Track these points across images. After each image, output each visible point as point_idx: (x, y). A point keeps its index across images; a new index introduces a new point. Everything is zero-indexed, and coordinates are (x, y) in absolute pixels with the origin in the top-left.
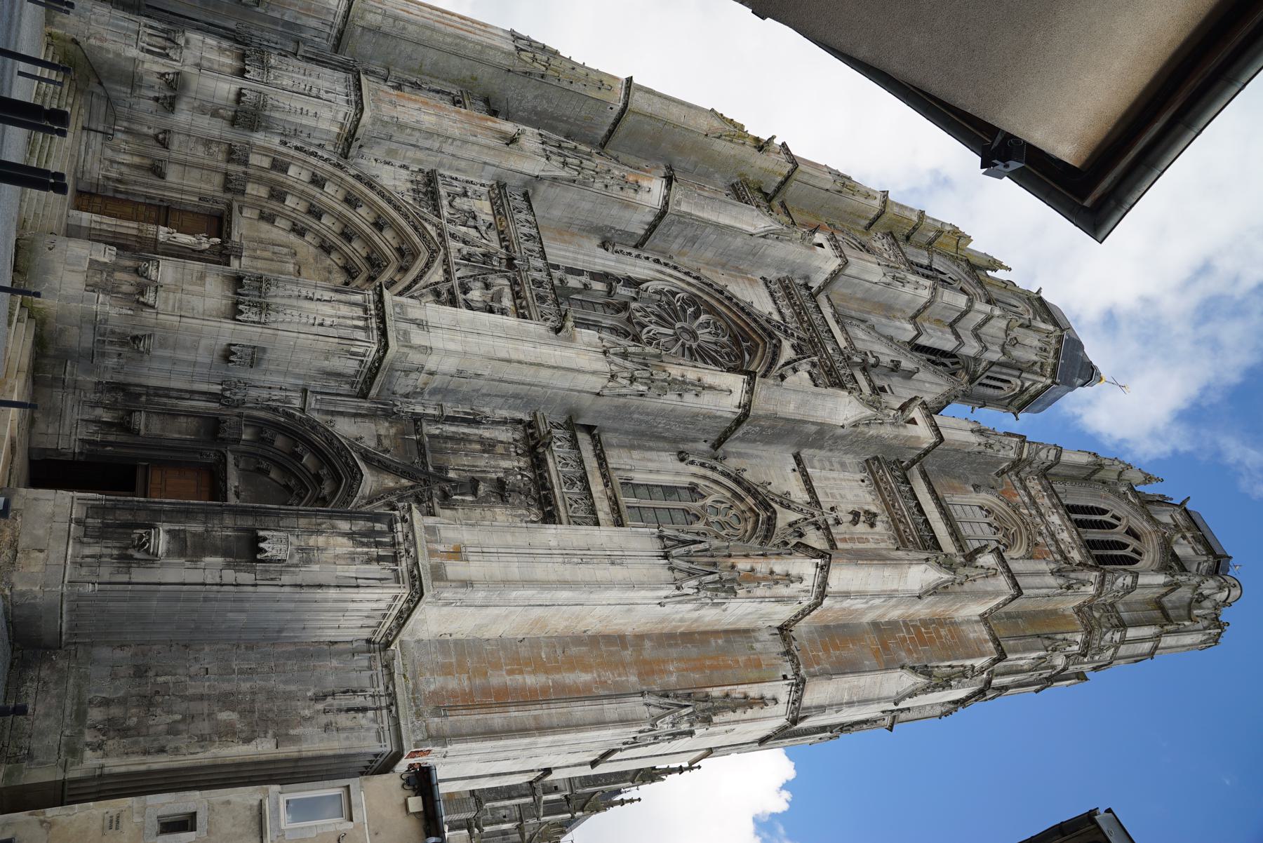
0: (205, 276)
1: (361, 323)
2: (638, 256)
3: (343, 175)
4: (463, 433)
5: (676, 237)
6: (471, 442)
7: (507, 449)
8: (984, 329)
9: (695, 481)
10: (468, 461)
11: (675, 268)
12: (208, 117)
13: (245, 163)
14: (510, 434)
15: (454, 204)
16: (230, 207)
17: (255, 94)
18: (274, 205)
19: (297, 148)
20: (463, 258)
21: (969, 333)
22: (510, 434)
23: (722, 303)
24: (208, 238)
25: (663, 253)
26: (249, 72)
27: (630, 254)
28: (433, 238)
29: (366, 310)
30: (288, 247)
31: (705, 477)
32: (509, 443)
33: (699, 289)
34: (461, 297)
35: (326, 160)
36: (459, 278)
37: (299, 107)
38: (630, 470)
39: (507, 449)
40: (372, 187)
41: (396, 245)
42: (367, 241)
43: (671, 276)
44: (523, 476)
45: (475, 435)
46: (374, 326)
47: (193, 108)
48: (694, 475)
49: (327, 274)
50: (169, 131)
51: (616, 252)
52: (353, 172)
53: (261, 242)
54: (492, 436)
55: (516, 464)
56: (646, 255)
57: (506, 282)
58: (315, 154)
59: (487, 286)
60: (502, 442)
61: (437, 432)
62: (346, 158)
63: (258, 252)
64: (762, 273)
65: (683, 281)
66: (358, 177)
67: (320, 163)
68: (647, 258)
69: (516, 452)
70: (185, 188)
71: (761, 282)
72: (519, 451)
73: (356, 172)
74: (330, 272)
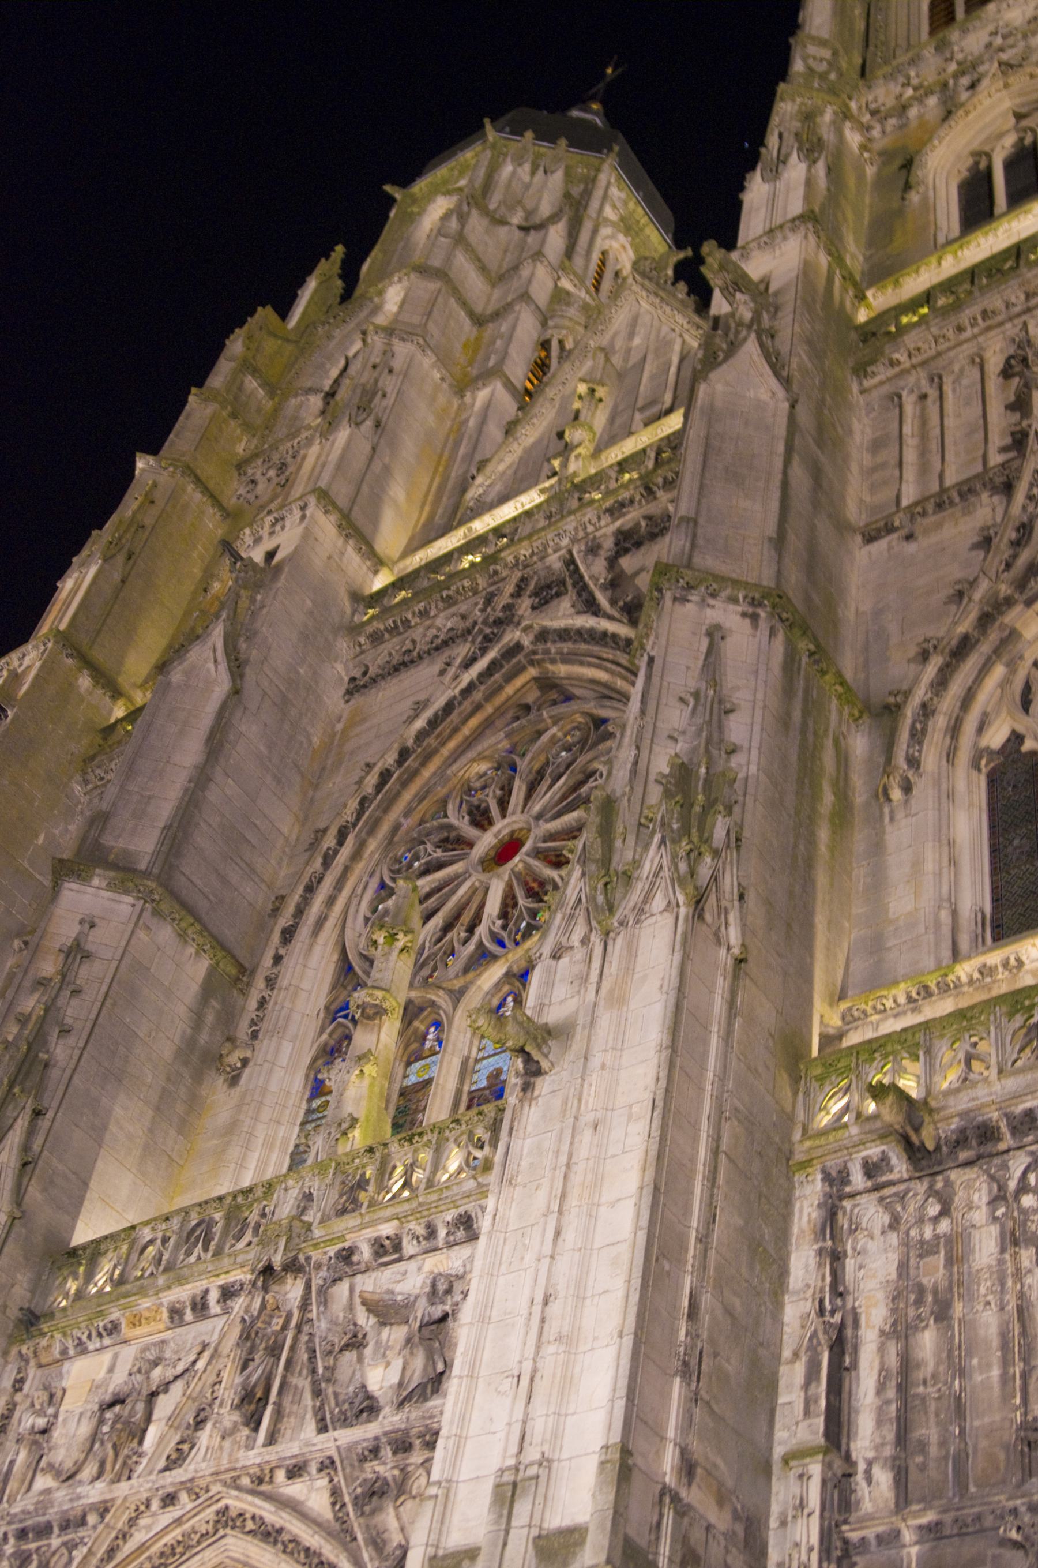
2: (271, 982)
4: (881, 1389)
5: (224, 880)
6: (907, 1364)
7: (927, 1249)
8: (493, 266)
9: (964, 755)
10: (988, 1366)
11: (310, 889)
14: (872, 1246)
15: (68, 1465)
20: (254, 1422)
21: (497, 294)
22: (872, 1246)
23: (414, 774)
25: (262, 928)
27: (262, 1003)
28: (178, 1521)
31: (955, 730)
32: (906, 1243)
33: (372, 831)
34: (389, 1420)
36: (323, 1429)
38: (954, 913)
39: (927, 1249)
43: (331, 901)
44: (1023, 1187)
45: (881, 1349)
48: (951, 755)
51: (255, 1035)
54: (880, 1295)
55: (980, 1216)
56: (267, 961)
57: (342, 1290)
59: (356, 1342)
60: (903, 1267)
61: (883, 1478)
64: (334, 700)
65: (346, 870)
68: (278, 959)
69: (936, 1220)
71: (358, 700)
72: (934, 1209)
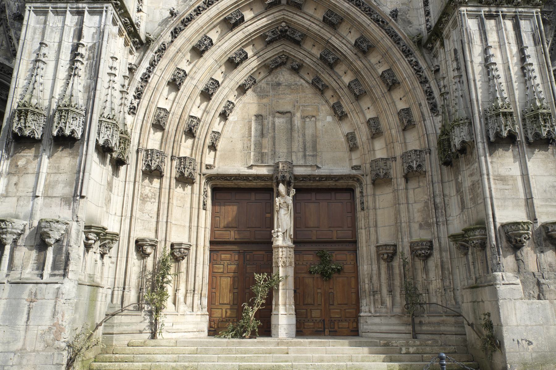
0: (499, 176)
1: (509, 24)
3: (172, 50)
12: (112, 196)
13: (161, 154)
16: (210, 178)
17: (103, 129)
18: (200, 132)
19: (139, 96)
24: (279, 195)
26: (73, 132)
29: (490, 16)
30: (250, 122)
35: (153, 65)
37: (107, 78)
40: (189, 20)
41: (263, 10)
42: (250, 40)
46: (514, 10)
47: (107, 212)
49: (281, 88)
50: (137, 242)
52: (167, 37)
53: (249, 148)
58: (145, 79)
62: (149, 41)
63: (266, 151)
66: (175, 33)
67: (157, 71)
70: (194, 223)
73: (169, 33)
74: (279, 84)
